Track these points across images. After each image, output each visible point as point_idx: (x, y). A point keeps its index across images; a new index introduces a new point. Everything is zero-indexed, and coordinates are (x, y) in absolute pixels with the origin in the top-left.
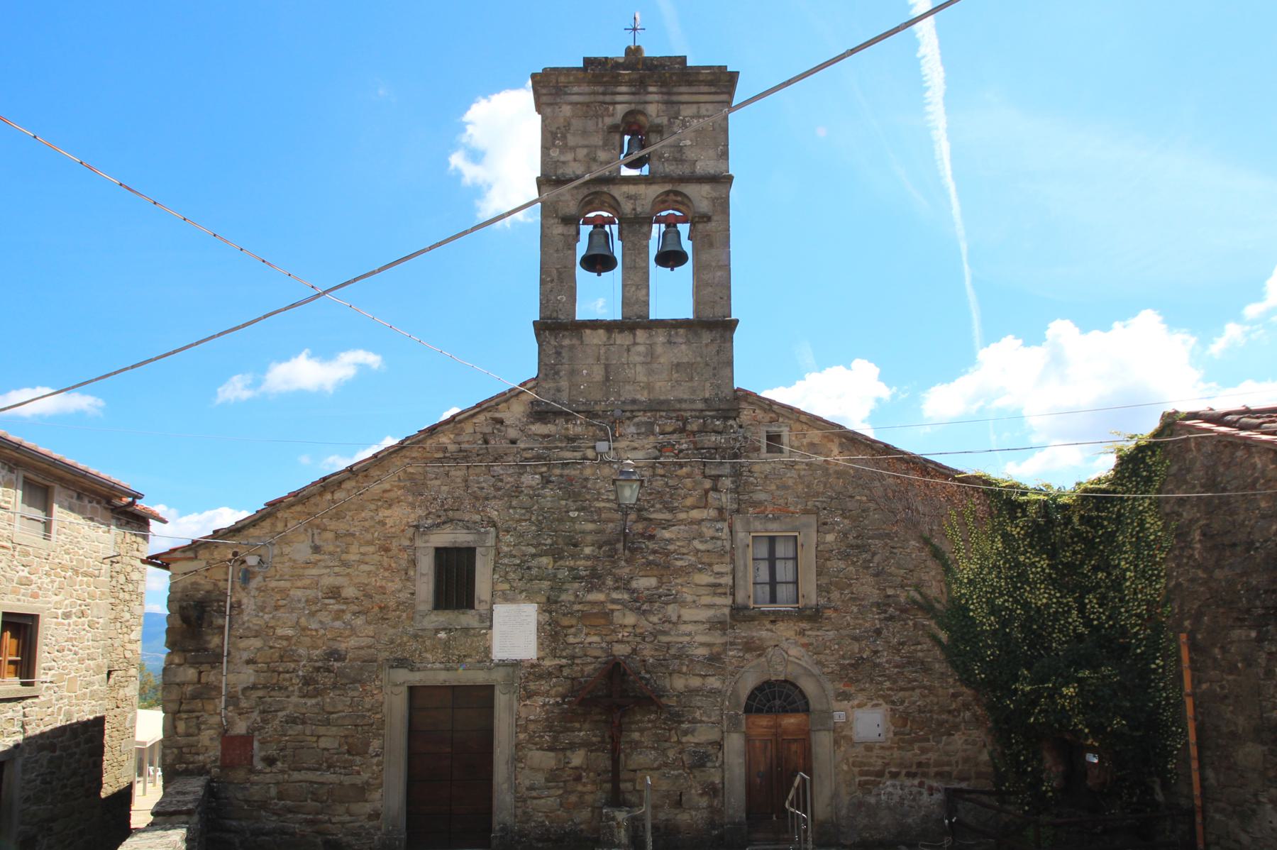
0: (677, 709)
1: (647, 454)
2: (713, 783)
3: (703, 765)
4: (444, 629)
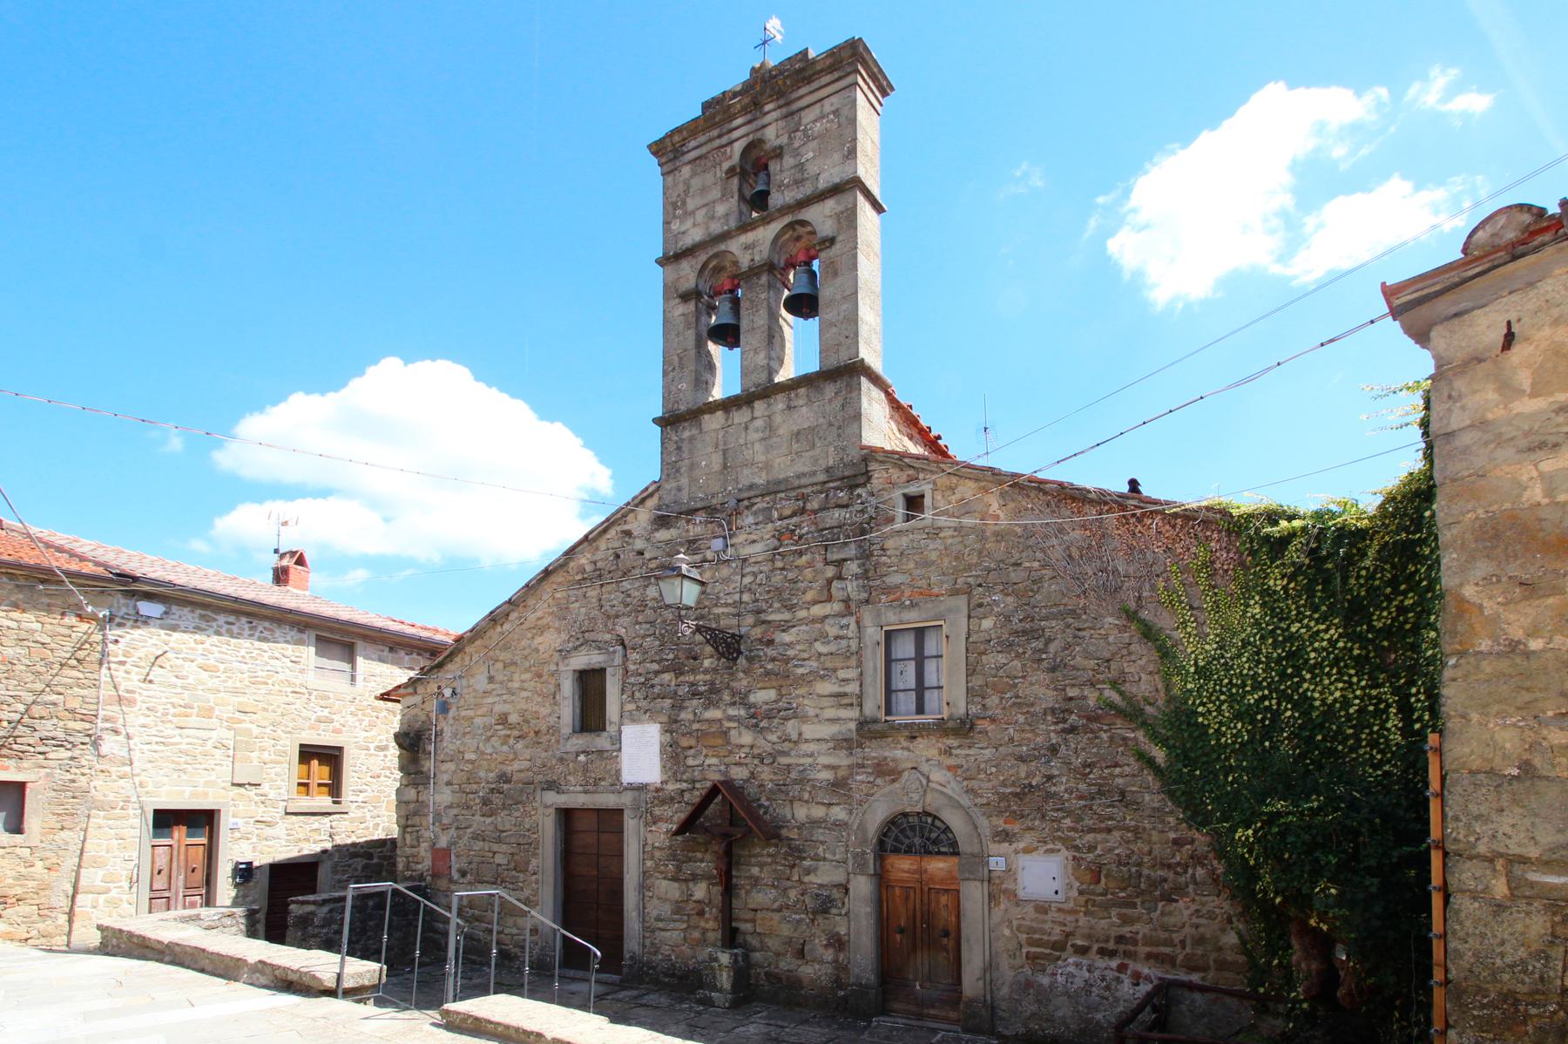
0: (797, 843)
1: (766, 545)
2: (838, 934)
3: (826, 911)
4: (583, 752)
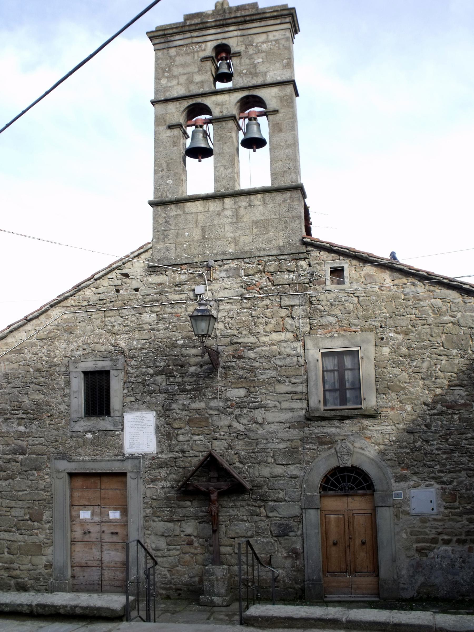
4: (90, 431)
